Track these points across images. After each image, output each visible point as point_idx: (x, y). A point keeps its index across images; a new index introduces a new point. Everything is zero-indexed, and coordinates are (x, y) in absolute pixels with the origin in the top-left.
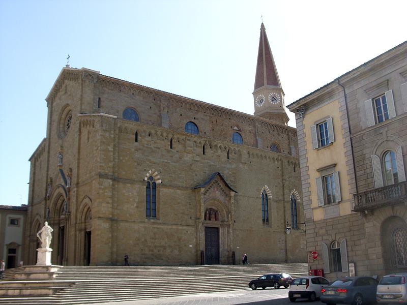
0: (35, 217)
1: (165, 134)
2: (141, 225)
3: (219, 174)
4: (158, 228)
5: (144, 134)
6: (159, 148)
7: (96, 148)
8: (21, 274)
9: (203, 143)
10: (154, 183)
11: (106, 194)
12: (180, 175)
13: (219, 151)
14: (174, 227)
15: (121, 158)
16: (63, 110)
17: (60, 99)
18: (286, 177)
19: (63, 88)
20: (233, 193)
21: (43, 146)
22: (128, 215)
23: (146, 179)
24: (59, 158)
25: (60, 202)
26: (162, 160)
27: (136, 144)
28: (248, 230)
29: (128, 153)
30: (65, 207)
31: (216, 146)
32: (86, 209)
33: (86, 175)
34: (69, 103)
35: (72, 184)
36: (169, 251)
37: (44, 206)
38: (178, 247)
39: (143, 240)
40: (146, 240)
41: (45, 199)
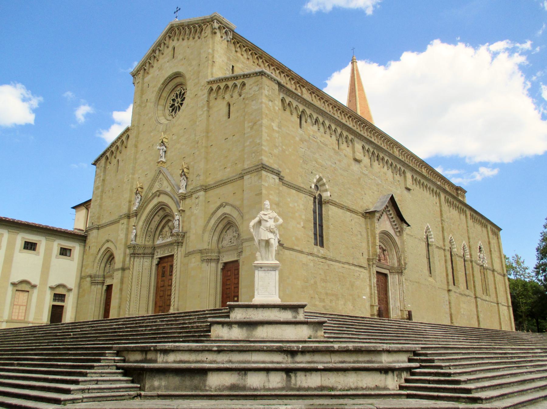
0: (103, 245)
1: (333, 127)
2: (310, 257)
3: (392, 199)
4: (328, 265)
5: (309, 120)
6: (326, 145)
7: (250, 124)
8: (230, 324)
9: (371, 150)
10: (320, 196)
12: (350, 191)
13: (386, 167)
14: (346, 266)
15: (284, 147)
16: (166, 83)
17: (160, 69)
18: (445, 216)
19: (165, 54)
20: (405, 226)
21: (124, 138)
22: (294, 238)
23: (313, 186)
24: (161, 151)
25: (157, 219)
26: (330, 163)
27: (300, 131)
28: (416, 282)
29: (292, 142)
30: (176, 223)
31: (383, 159)
32: (221, 226)
34: (181, 69)
35: (189, 188)
36: (342, 303)
37: (125, 226)
38: (351, 297)
39: (312, 282)
40: (315, 283)
41: (128, 217)
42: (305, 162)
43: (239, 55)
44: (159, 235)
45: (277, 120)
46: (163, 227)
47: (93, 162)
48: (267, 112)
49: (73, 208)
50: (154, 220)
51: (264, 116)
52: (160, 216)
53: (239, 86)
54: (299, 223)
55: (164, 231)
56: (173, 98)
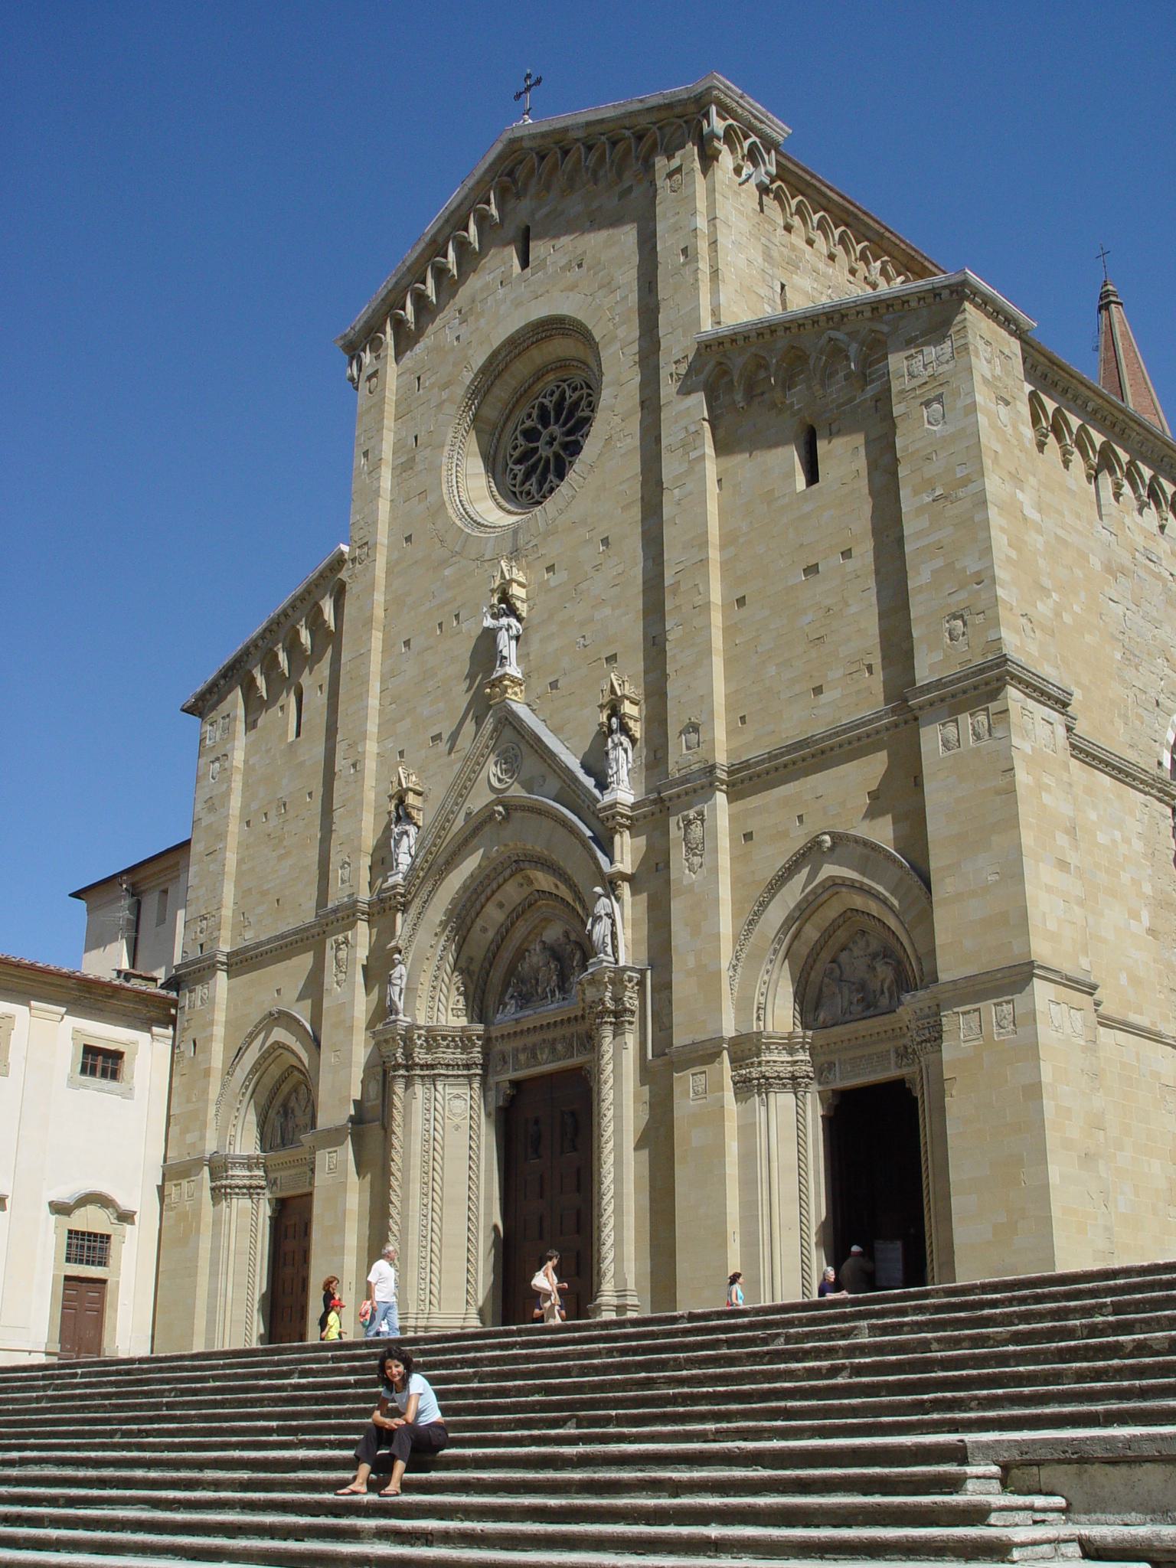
11: (1046, 798)
22: (1123, 979)
29: (1079, 573)
33: (818, 690)
42: (1131, 658)
43: (797, 240)
44: (506, 984)
45: (1032, 481)
46: (521, 954)
47: (189, 698)
48: (998, 447)
49: (77, 895)
50: (479, 922)
51: (988, 462)
52: (509, 908)
53: (853, 348)
54: (1135, 915)
55: (524, 968)
56: (529, 424)
